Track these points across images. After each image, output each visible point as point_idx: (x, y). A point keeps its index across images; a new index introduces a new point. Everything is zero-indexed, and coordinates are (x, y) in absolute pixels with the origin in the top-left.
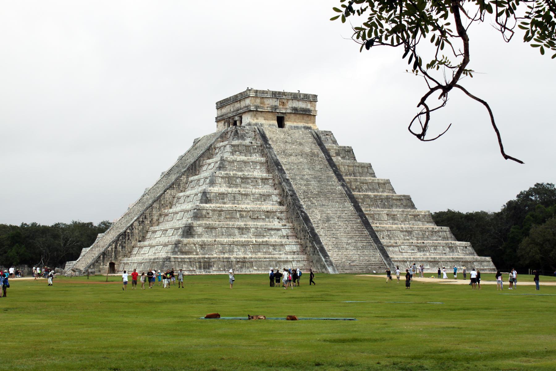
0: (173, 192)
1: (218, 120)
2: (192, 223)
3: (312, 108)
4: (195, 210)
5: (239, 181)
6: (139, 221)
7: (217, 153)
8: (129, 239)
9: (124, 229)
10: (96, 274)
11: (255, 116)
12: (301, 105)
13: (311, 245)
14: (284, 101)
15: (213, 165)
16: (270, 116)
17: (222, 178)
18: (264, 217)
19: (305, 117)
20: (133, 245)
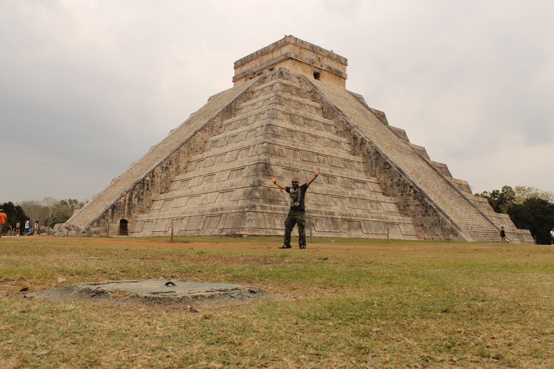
0: (205, 135)
1: (235, 79)
2: (269, 159)
3: (343, 71)
4: (265, 144)
5: (301, 120)
6: (163, 167)
7: (257, 97)
8: (148, 189)
9: (142, 176)
10: (101, 234)
11: (294, 64)
12: (335, 66)
13: (417, 202)
14: (319, 56)
15: (261, 104)
16: (308, 69)
17: (284, 113)
18: (342, 166)
19: (338, 78)
20: (152, 197)
